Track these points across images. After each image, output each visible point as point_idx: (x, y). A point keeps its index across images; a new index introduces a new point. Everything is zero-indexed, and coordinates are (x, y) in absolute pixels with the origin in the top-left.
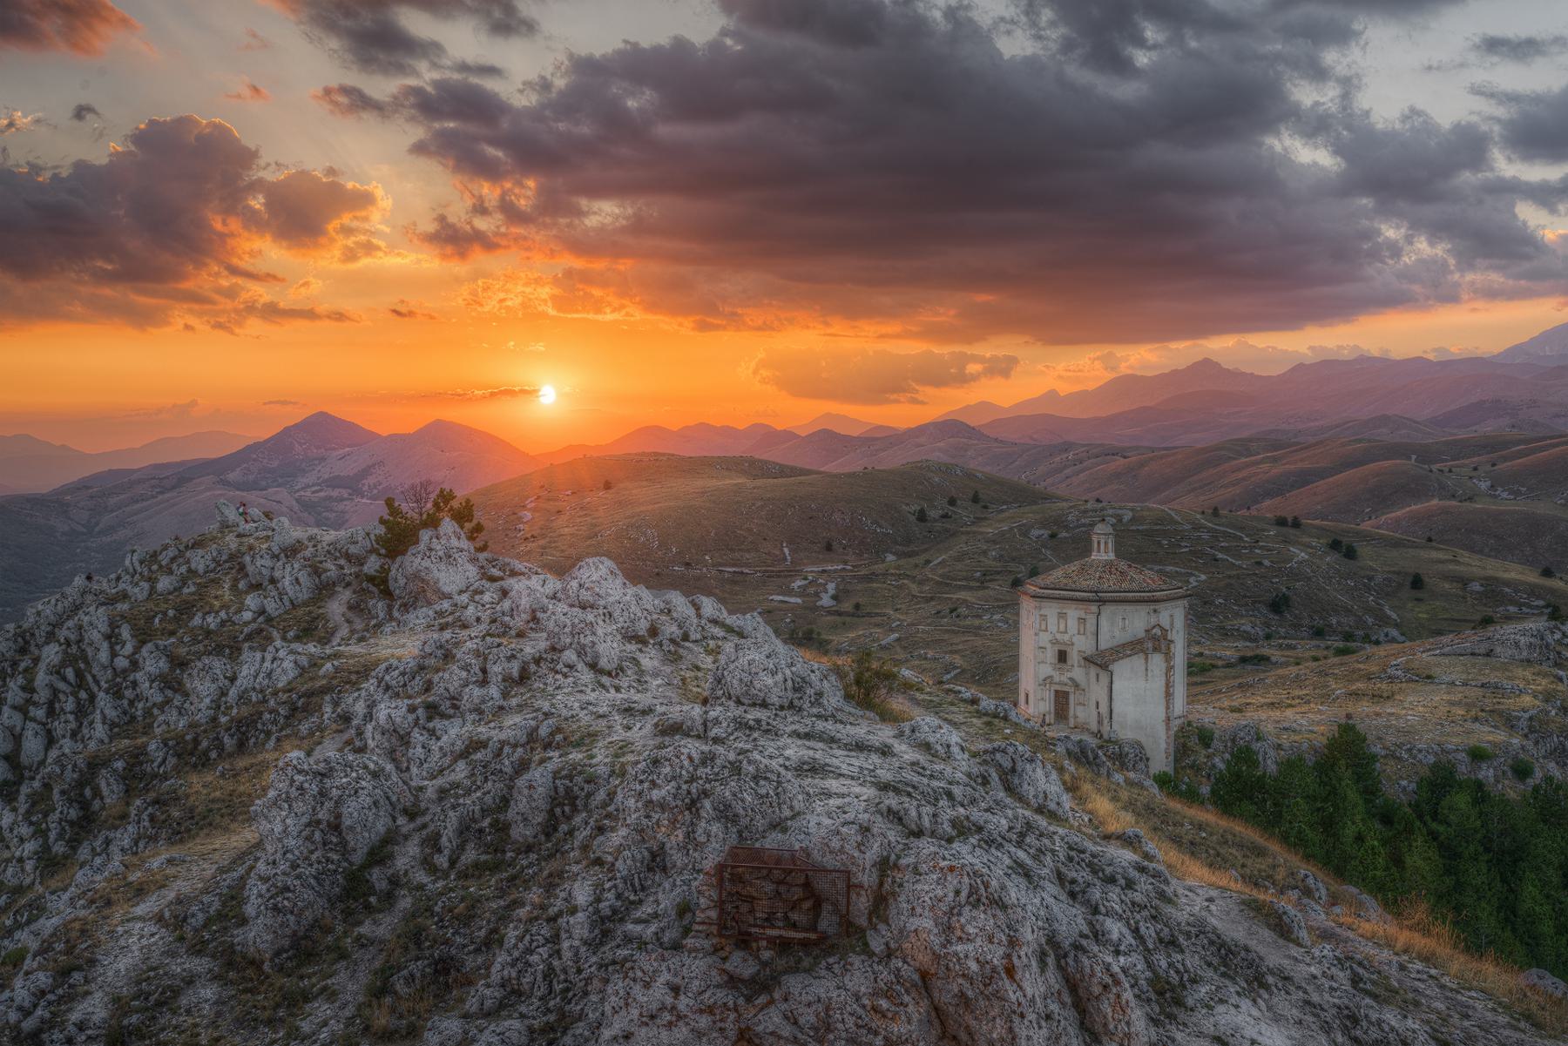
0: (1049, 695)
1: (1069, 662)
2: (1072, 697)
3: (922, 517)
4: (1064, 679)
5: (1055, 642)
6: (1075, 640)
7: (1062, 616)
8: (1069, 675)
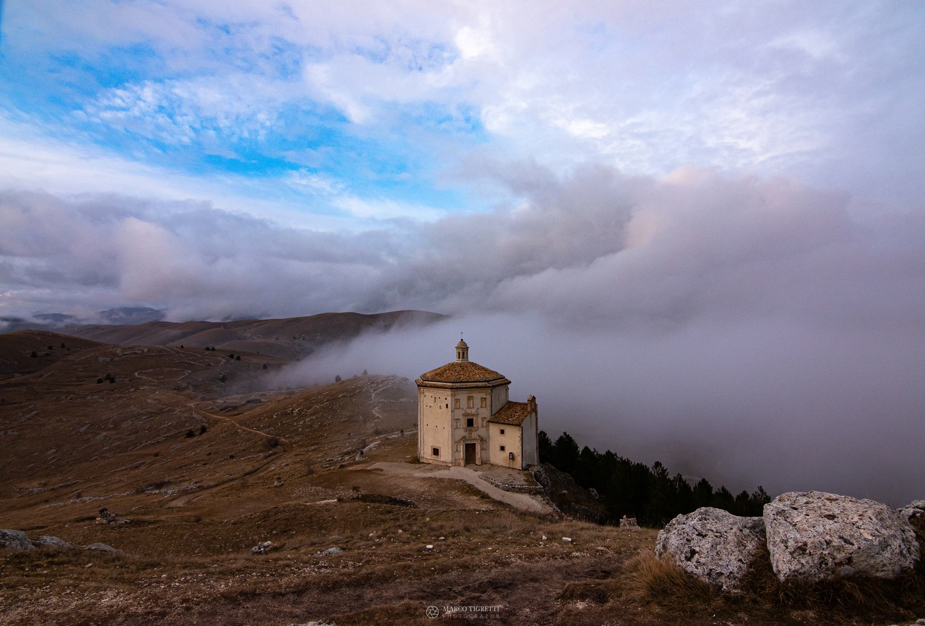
0: (462, 448)
2: (478, 448)
3: (34, 355)
5: (465, 415)
7: (470, 398)
8: (476, 433)
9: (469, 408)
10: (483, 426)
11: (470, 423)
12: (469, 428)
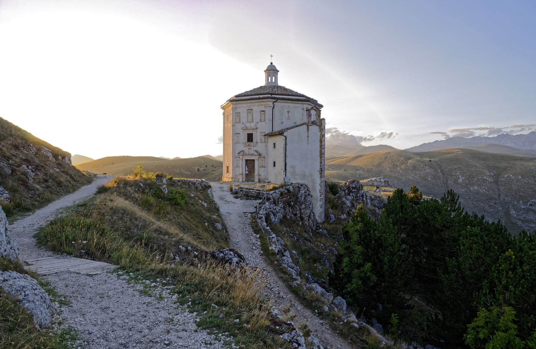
0: (242, 163)
1: (254, 140)
3: (198, 170)
4: (252, 152)
5: (244, 129)
6: (258, 125)
8: (255, 148)
9: (248, 122)
10: (261, 142)
11: (250, 138)
12: (249, 143)
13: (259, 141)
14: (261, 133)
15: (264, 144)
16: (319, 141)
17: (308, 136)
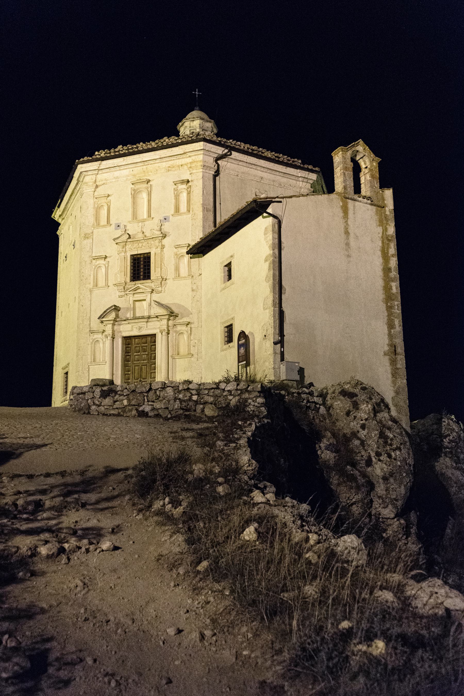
4: (143, 309)
11: (141, 268)
13: (170, 273)
14: (177, 247)
15: (189, 281)
16: (379, 253)
17: (347, 233)
